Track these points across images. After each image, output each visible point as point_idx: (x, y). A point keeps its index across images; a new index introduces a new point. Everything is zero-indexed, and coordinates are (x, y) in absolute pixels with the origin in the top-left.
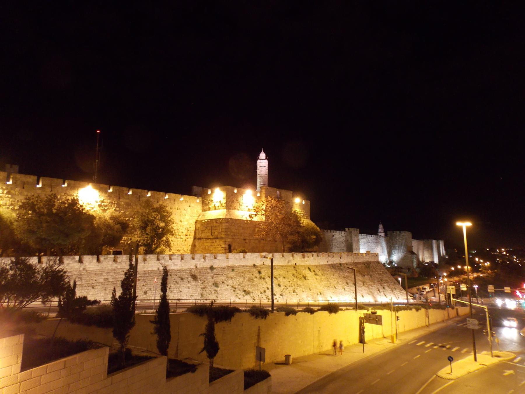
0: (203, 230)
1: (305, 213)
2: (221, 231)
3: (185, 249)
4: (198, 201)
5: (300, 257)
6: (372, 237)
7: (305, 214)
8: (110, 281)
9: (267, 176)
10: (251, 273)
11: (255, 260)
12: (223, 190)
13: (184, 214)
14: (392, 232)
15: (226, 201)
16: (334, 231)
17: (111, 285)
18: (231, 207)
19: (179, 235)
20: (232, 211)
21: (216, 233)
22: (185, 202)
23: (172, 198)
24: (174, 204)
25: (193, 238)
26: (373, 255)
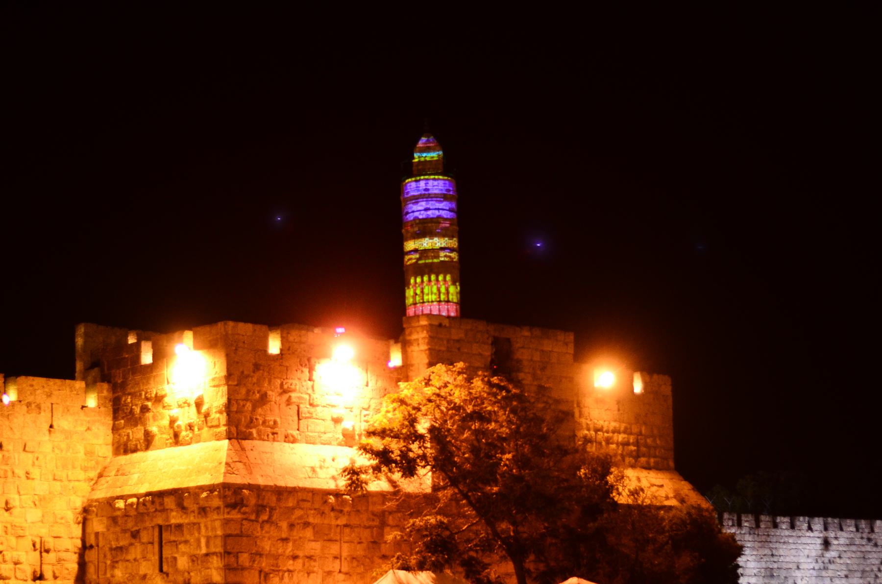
0: (120, 549)
2: (204, 551)
4: (92, 401)
12: (211, 345)
15: (229, 400)
16: (830, 520)
18: (255, 427)
20: (257, 447)
21: (183, 562)
22: (25, 408)
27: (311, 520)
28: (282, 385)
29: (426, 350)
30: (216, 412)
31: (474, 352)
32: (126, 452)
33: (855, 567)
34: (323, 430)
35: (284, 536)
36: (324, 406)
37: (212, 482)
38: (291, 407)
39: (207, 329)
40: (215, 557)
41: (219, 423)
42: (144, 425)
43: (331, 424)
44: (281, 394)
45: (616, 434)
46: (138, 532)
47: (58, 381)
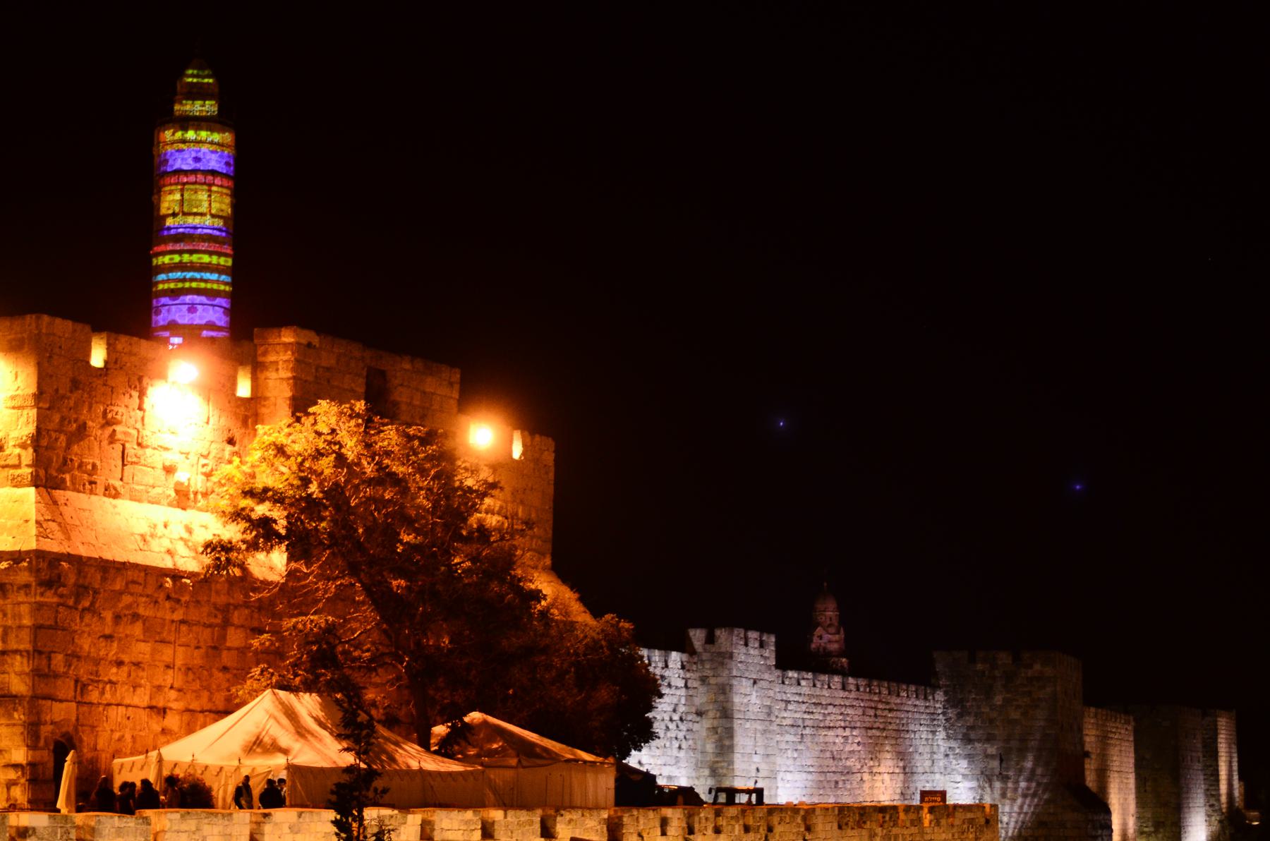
6: (844, 688)
15: (38, 429)
20: (73, 500)
26: (969, 815)
27: (141, 611)
28: (105, 413)
29: (289, 379)
30: (14, 446)
31: (346, 387)
34: (151, 482)
35: (107, 631)
36: (155, 449)
37: (17, 548)
38: (114, 446)
40: (18, 657)
41: (20, 463)
43: (160, 473)
44: (103, 427)
45: (489, 516)
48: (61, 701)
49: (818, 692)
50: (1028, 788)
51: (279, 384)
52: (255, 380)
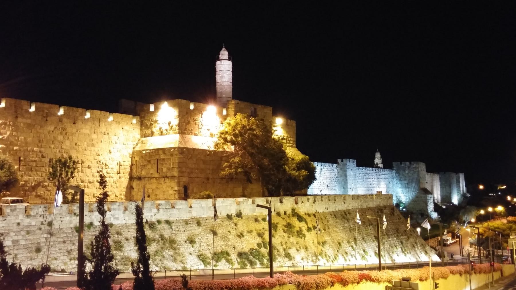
0: (144, 165)
1: (290, 139)
2: (172, 166)
3: (118, 194)
4: (134, 121)
5: (292, 203)
6: (372, 170)
7: (289, 140)
8: (21, 244)
9: (231, 84)
10: (224, 228)
11: (228, 208)
12: (174, 106)
13: (114, 143)
14: (399, 163)
15: (179, 122)
16: (322, 163)
17: (23, 250)
18: (186, 131)
19: (107, 173)
20: (187, 136)
21: (165, 170)
23: (96, 117)
24: (99, 126)
25: (128, 177)
26: (385, 196)
28: (194, 119)
32: (145, 137)
33: (328, 177)
39: (172, 101)
42: (151, 129)
44: (193, 121)
46: (150, 160)
47: (125, 115)
48: (185, 177)
49: (366, 171)
50: (414, 190)
51: (232, 111)
52: (227, 110)
